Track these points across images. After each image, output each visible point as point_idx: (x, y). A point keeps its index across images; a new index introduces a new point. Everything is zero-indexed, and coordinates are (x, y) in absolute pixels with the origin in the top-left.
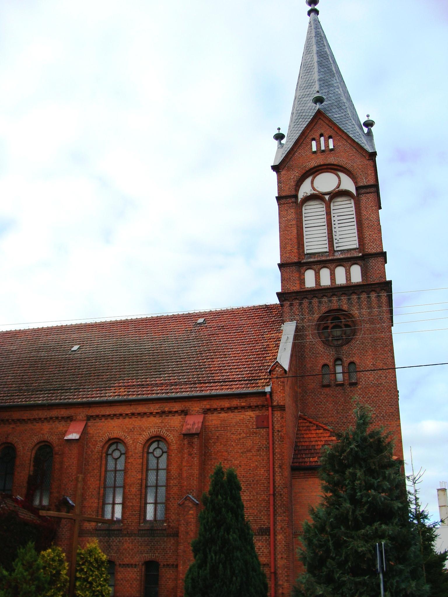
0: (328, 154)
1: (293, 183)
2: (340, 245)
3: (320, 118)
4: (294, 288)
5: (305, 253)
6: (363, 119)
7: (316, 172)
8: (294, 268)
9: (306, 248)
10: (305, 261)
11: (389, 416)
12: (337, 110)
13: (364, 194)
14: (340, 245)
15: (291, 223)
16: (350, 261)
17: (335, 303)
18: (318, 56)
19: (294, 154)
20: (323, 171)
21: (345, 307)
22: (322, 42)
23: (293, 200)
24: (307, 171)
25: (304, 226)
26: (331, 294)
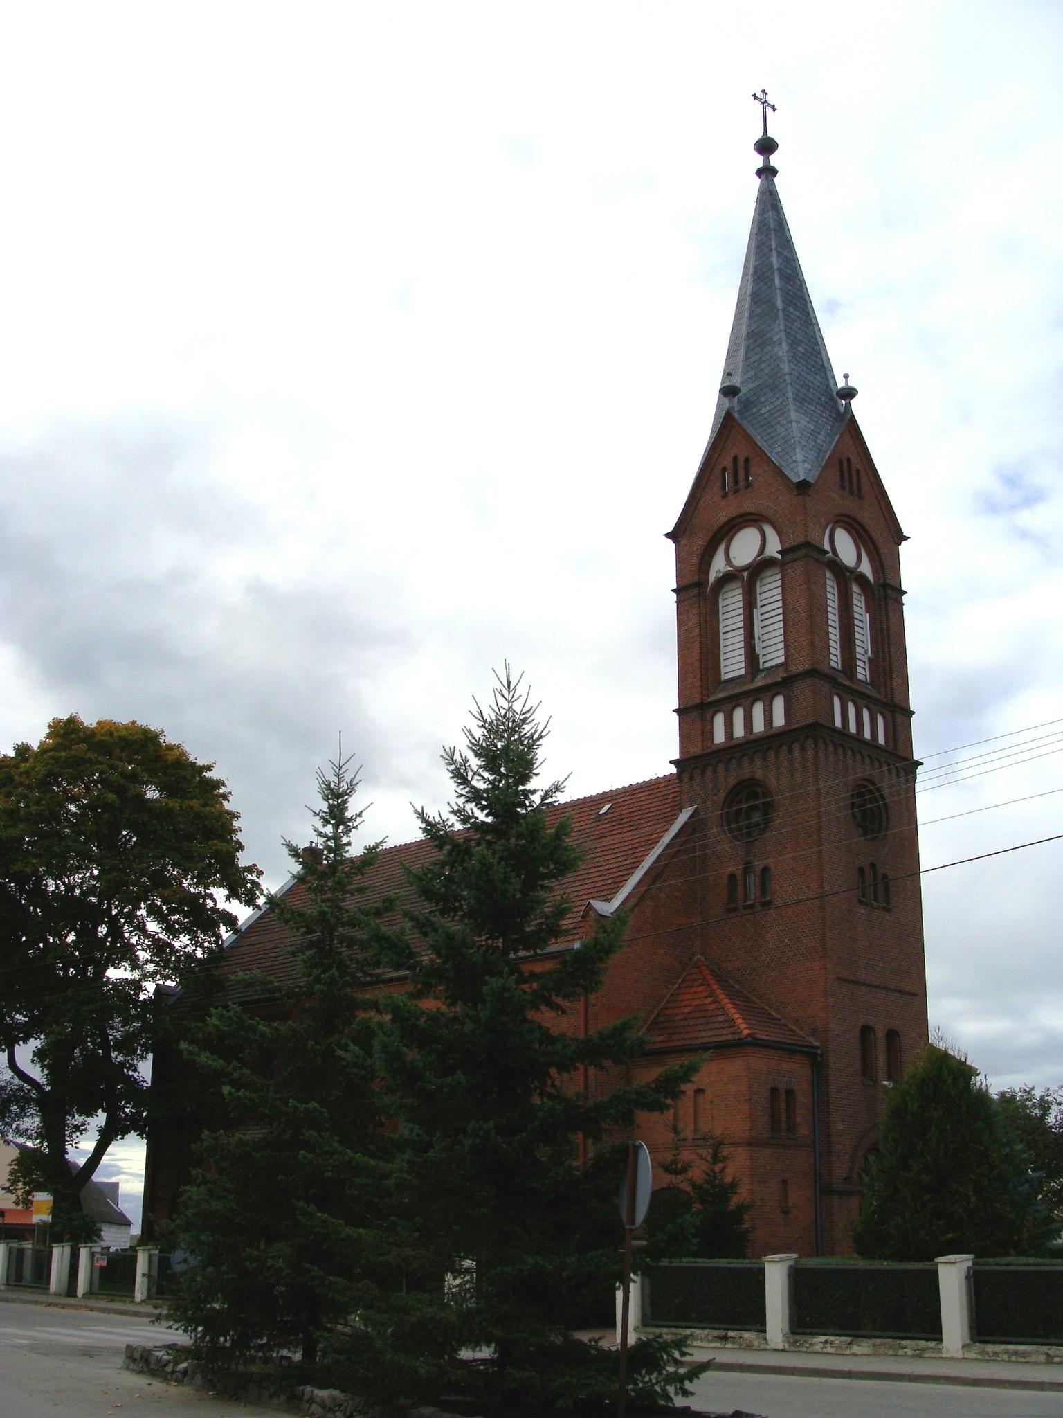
1: (695, 560)
2: (769, 657)
3: (732, 426)
4: (696, 749)
6: (841, 383)
7: (731, 529)
9: (723, 670)
10: (711, 699)
13: (789, 562)
14: (769, 657)
17: (745, 770)
19: (697, 503)
21: (759, 774)
23: (696, 591)
24: (715, 534)
25: (721, 630)
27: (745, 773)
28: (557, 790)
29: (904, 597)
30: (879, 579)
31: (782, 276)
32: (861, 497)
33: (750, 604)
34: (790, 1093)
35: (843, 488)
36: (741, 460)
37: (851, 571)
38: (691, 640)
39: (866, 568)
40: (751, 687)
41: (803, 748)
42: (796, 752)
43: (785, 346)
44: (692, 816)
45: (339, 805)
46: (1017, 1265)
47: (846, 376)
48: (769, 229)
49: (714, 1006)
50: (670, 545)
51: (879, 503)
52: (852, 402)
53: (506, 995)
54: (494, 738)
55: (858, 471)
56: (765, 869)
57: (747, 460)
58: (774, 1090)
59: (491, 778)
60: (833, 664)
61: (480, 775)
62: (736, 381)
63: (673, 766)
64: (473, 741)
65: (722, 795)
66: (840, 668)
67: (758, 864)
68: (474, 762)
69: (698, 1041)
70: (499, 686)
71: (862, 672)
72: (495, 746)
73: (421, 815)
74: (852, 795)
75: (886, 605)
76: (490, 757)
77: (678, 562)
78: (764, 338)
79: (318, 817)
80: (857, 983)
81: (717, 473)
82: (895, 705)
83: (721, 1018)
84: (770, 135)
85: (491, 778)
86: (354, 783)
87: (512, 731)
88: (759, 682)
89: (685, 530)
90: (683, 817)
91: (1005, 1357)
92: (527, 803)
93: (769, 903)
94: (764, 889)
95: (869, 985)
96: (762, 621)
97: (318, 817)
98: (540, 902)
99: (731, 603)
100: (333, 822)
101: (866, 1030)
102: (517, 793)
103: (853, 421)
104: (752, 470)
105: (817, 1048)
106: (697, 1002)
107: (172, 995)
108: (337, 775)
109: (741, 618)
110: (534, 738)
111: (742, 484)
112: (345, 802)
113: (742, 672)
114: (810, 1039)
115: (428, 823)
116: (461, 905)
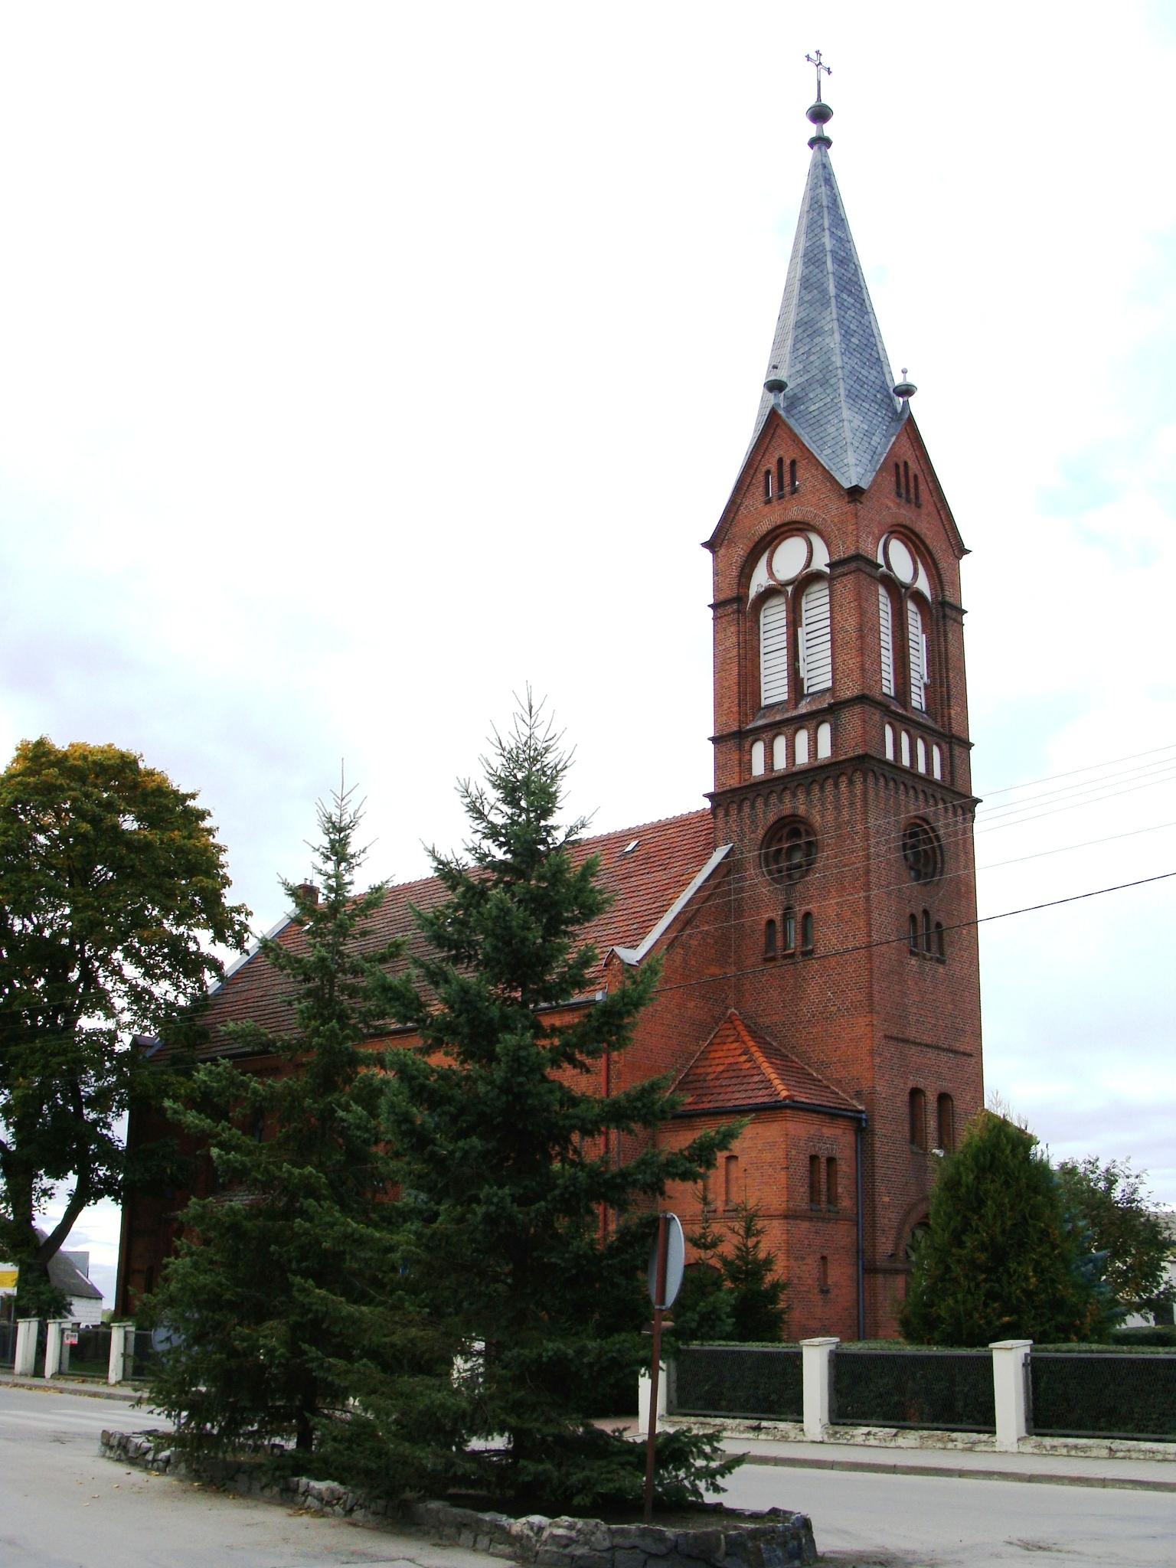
0: (789, 500)
2: (813, 681)
3: (778, 425)
4: (732, 782)
5: (763, 705)
6: (898, 379)
7: (775, 538)
8: (731, 743)
10: (751, 726)
11: (856, 1008)
12: (820, 390)
13: (838, 577)
14: (813, 681)
15: (730, 655)
16: (814, 718)
17: (789, 804)
18: (804, 263)
19: (738, 510)
20: (786, 535)
21: (802, 810)
22: (819, 223)
23: (735, 606)
24: (757, 544)
26: (782, 787)
27: (787, 808)
28: (583, 826)
29: (965, 617)
30: (937, 596)
31: (835, 259)
32: (918, 506)
33: (794, 622)
34: (831, 1160)
35: (899, 495)
36: (787, 462)
37: (907, 587)
38: (729, 661)
39: (923, 585)
40: (795, 713)
41: (851, 782)
42: (843, 787)
43: (837, 337)
44: (727, 856)
45: (341, 840)
46: (1080, 1352)
47: (904, 372)
48: (821, 206)
49: (749, 1065)
50: (707, 555)
51: (938, 511)
52: (911, 399)
53: (523, 1053)
54: (514, 768)
55: (916, 477)
56: (808, 915)
57: (793, 463)
58: (814, 1158)
59: (510, 811)
60: (885, 690)
61: (497, 809)
62: (782, 375)
63: (707, 799)
64: (491, 771)
65: (761, 832)
66: (892, 694)
67: (800, 910)
68: (493, 795)
69: (730, 1104)
70: (521, 711)
71: (918, 699)
72: (515, 776)
73: (432, 853)
74: (904, 835)
75: (945, 625)
76: (511, 791)
77: (716, 574)
78: (815, 327)
79: (318, 853)
80: (906, 1041)
81: (760, 477)
82: (953, 736)
83: (756, 1079)
84: (824, 101)
85: (510, 811)
86: (358, 815)
87: (534, 760)
88: (804, 708)
89: (724, 539)
90: (718, 856)
91: (1064, 1451)
92: (550, 840)
93: (812, 952)
94: (805, 937)
95: (919, 1044)
96: (807, 641)
97: (318, 853)
98: (562, 949)
99: (774, 619)
100: (334, 858)
101: (916, 1093)
102: (538, 830)
103: (911, 421)
104: (799, 474)
105: (861, 1112)
106: (731, 1060)
107: (151, 1047)
108: (339, 807)
109: (784, 637)
110: (558, 769)
111: (787, 489)
112: (347, 836)
113: (785, 697)
114: (854, 1102)
115: (440, 862)
116: (476, 954)
